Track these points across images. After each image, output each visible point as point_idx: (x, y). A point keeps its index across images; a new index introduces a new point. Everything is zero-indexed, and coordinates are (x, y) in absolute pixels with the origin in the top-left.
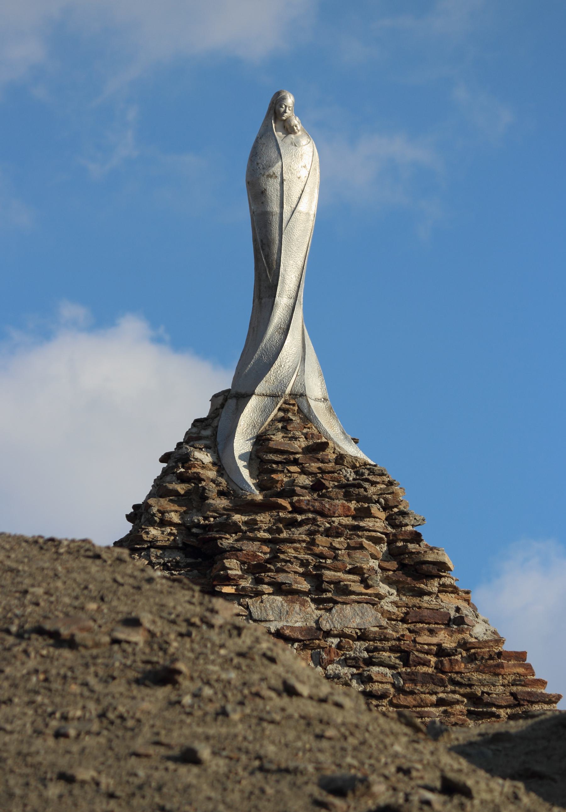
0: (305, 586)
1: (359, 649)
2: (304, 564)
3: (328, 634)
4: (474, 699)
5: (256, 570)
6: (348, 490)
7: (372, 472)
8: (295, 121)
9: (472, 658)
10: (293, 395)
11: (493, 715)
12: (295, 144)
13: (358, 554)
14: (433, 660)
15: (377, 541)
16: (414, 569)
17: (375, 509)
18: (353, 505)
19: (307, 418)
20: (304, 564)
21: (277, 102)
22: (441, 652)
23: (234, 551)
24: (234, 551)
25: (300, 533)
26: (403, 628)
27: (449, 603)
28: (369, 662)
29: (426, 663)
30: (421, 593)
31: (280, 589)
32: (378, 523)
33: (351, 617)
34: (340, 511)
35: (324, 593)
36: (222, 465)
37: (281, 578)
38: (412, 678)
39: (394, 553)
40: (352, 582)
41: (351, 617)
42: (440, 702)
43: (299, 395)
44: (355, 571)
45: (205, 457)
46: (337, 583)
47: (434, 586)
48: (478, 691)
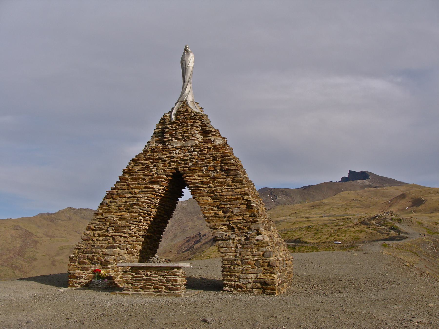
0: (181, 137)
1: (192, 149)
2: (181, 133)
3: (185, 147)
4: (214, 157)
5: (171, 135)
6: (191, 118)
7: (197, 114)
8: (189, 50)
9: (214, 149)
10: (185, 101)
11: (217, 160)
12: (189, 54)
13: (192, 130)
14: (206, 150)
15: (198, 127)
16: (205, 132)
17: (197, 121)
18: (193, 121)
19: (187, 105)
20: (181, 133)
21: (186, 47)
22: (208, 148)
23: (167, 132)
24: (167, 132)
25: (180, 127)
26: (202, 144)
27: (213, 138)
28: (193, 152)
29: (205, 151)
30: (208, 137)
31: (176, 139)
32: (198, 123)
33: (190, 143)
34: (189, 122)
35: (185, 138)
36: (170, 116)
37: (176, 136)
38: (200, 154)
39: (202, 129)
40: (190, 136)
41: (190, 143)
42: (206, 159)
43: (186, 101)
44: (191, 134)
45: (168, 115)
46: (187, 136)
47: (210, 135)
48: (214, 155)
